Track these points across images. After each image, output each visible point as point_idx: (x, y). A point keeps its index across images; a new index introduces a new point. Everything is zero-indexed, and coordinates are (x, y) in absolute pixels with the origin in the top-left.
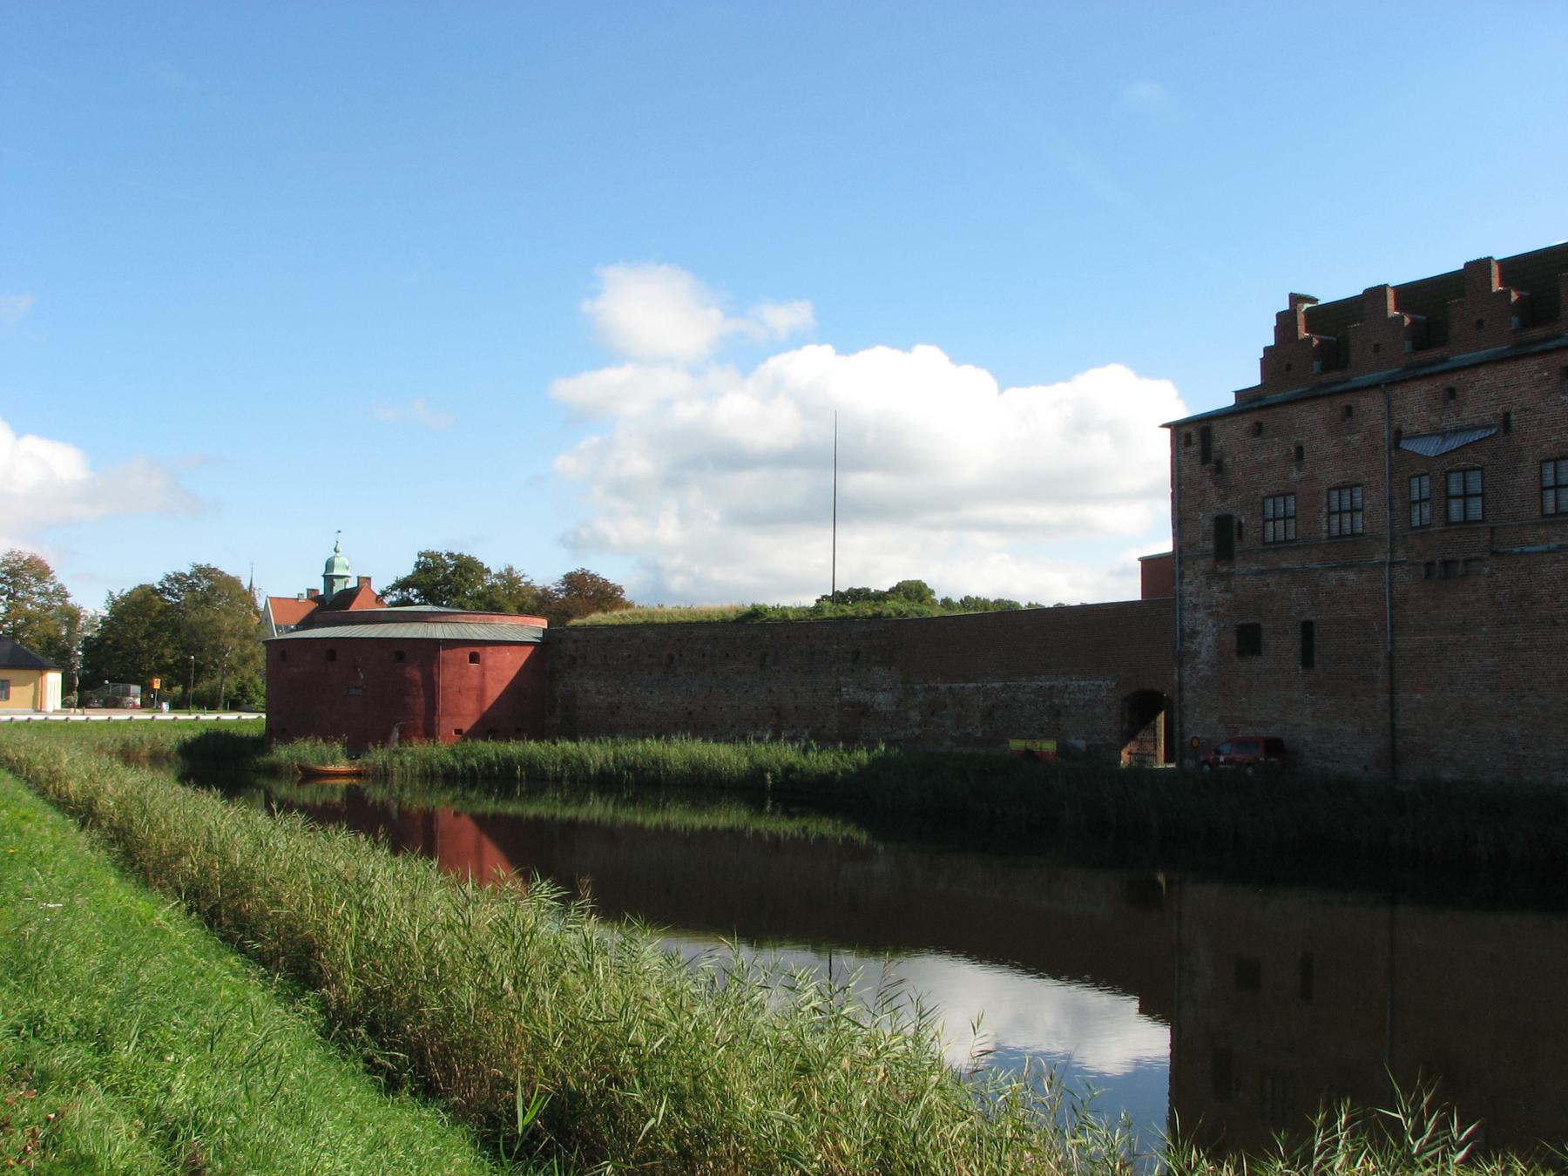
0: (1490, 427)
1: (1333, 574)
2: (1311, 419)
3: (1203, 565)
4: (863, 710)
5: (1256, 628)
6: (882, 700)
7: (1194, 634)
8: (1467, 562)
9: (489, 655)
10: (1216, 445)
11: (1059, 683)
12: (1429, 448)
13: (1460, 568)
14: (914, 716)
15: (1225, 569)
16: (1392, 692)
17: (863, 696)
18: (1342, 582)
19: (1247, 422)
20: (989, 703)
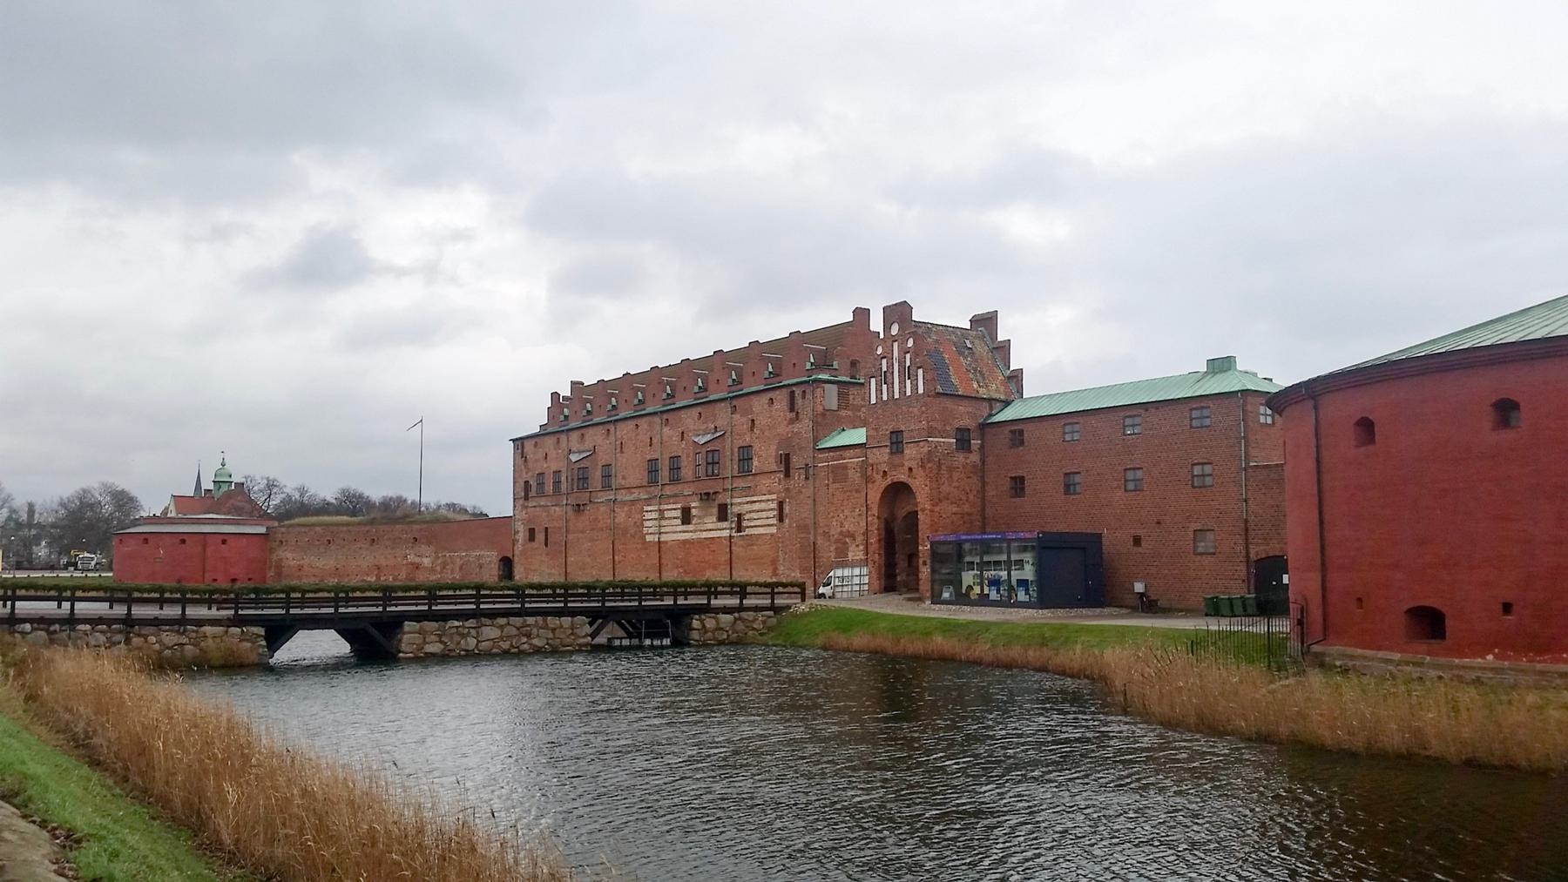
0: (590, 451)
1: (553, 508)
2: (550, 441)
3: (521, 501)
4: (417, 567)
5: (534, 529)
6: (426, 561)
7: (516, 532)
8: (583, 505)
9: (231, 541)
10: (525, 451)
11: (482, 553)
12: (574, 458)
13: (582, 508)
14: (438, 568)
15: (526, 504)
16: (566, 557)
17: (417, 560)
18: (555, 510)
19: (533, 441)
20: (462, 562)
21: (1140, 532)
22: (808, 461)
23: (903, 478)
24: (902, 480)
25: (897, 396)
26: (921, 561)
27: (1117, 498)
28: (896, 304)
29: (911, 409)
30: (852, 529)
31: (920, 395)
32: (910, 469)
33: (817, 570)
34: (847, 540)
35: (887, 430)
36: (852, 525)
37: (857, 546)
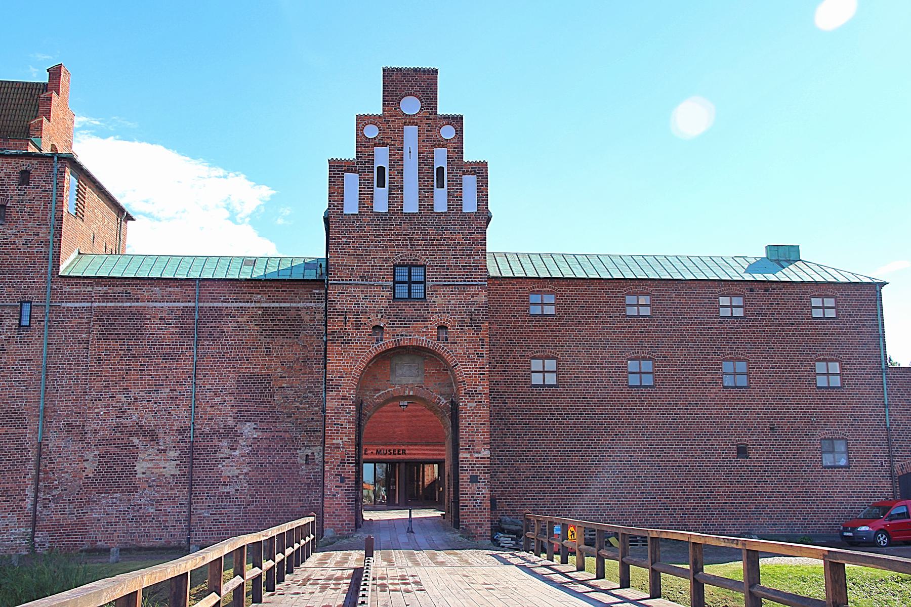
21: (745, 439)
22: (30, 294)
23: (423, 340)
24: (420, 343)
25: (411, 205)
26: (464, 477)
27: (713, 396)
28: (415, 70)
29: (447, 234)
30: (149, 420)
31: (469, 215)
32: (442, 327)
33: (41, 495)
34: (135, 440)
35: (386, 260)
36: (149, 416)
37: (164, 451)
